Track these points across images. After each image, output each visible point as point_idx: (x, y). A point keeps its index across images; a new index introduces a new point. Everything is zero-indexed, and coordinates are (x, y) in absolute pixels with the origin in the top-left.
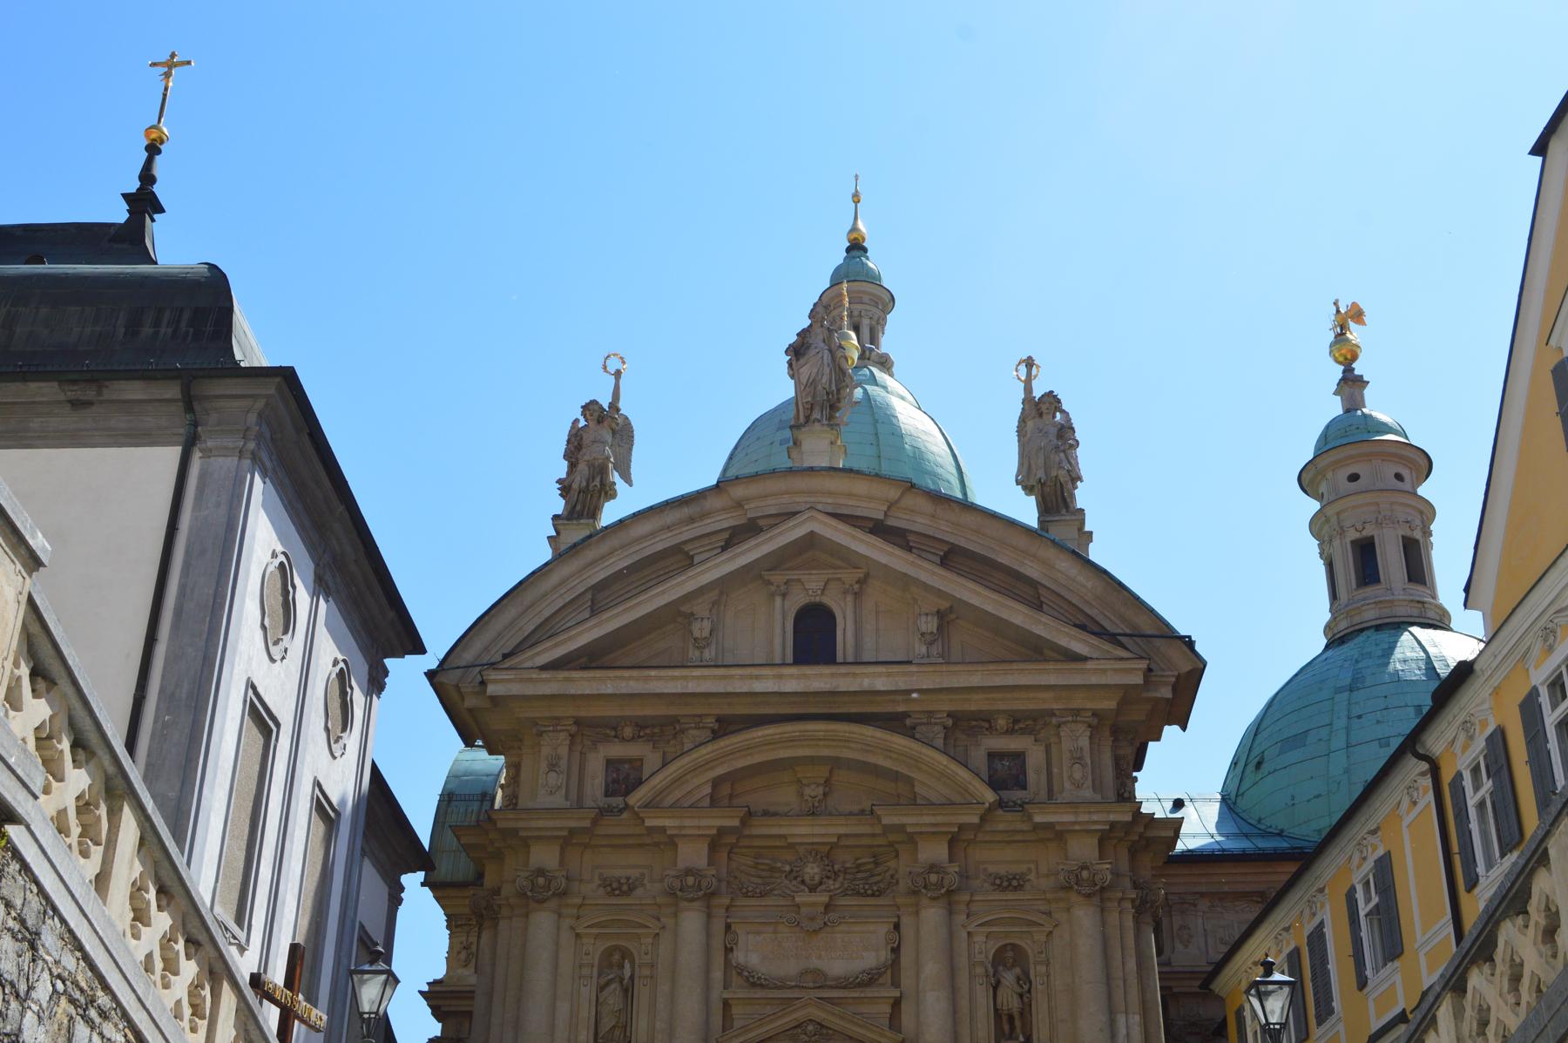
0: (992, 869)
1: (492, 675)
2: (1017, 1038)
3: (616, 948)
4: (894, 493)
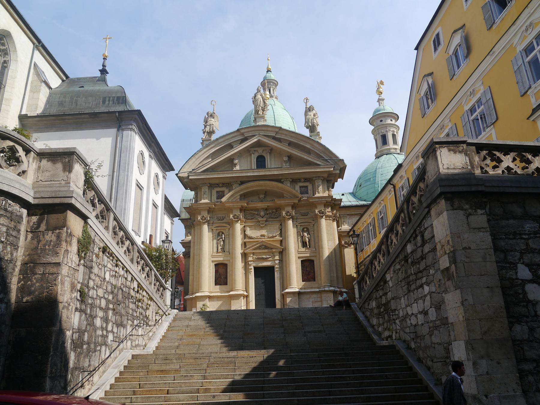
0: (301, 211)
4: (277, 130)
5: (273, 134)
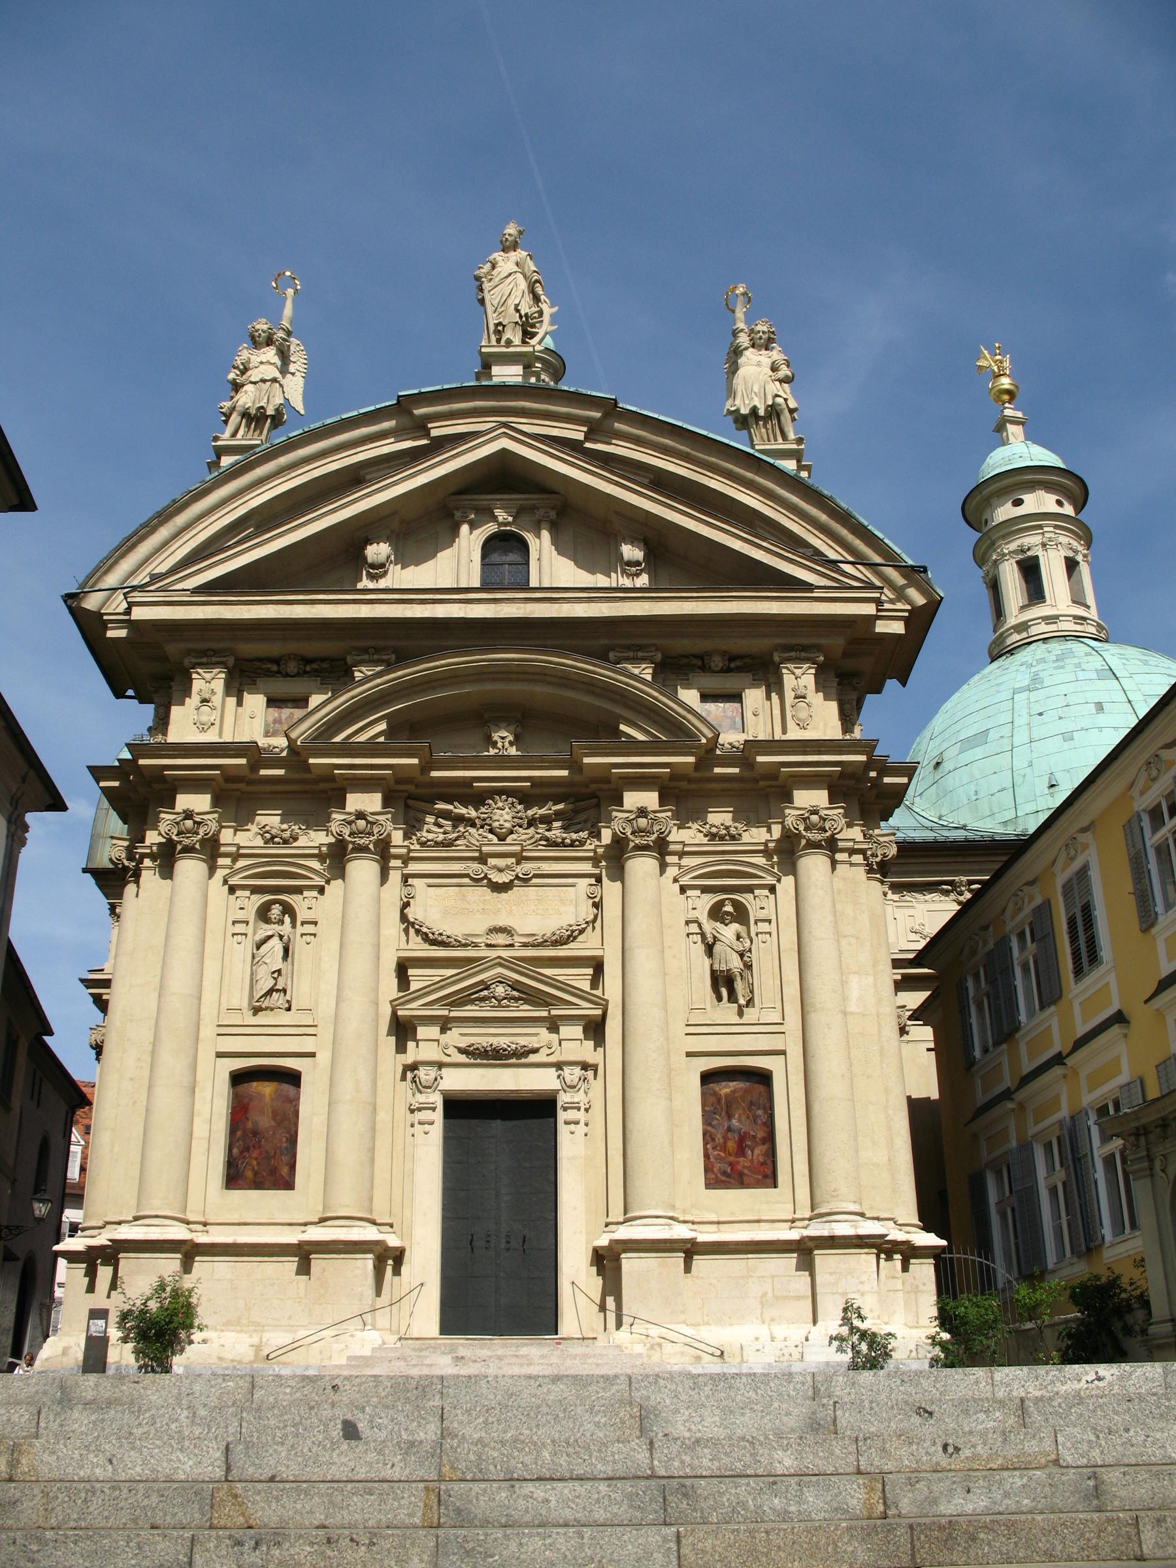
1: (137, 597)
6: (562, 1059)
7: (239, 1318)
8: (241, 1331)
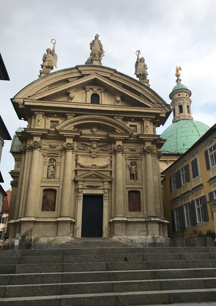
2: (135, 179)
3: (52, 159)
4: (113, 72)
5: (108, 76)
6: (104, 188)
7: (44, 235)
8: (45, 237)
